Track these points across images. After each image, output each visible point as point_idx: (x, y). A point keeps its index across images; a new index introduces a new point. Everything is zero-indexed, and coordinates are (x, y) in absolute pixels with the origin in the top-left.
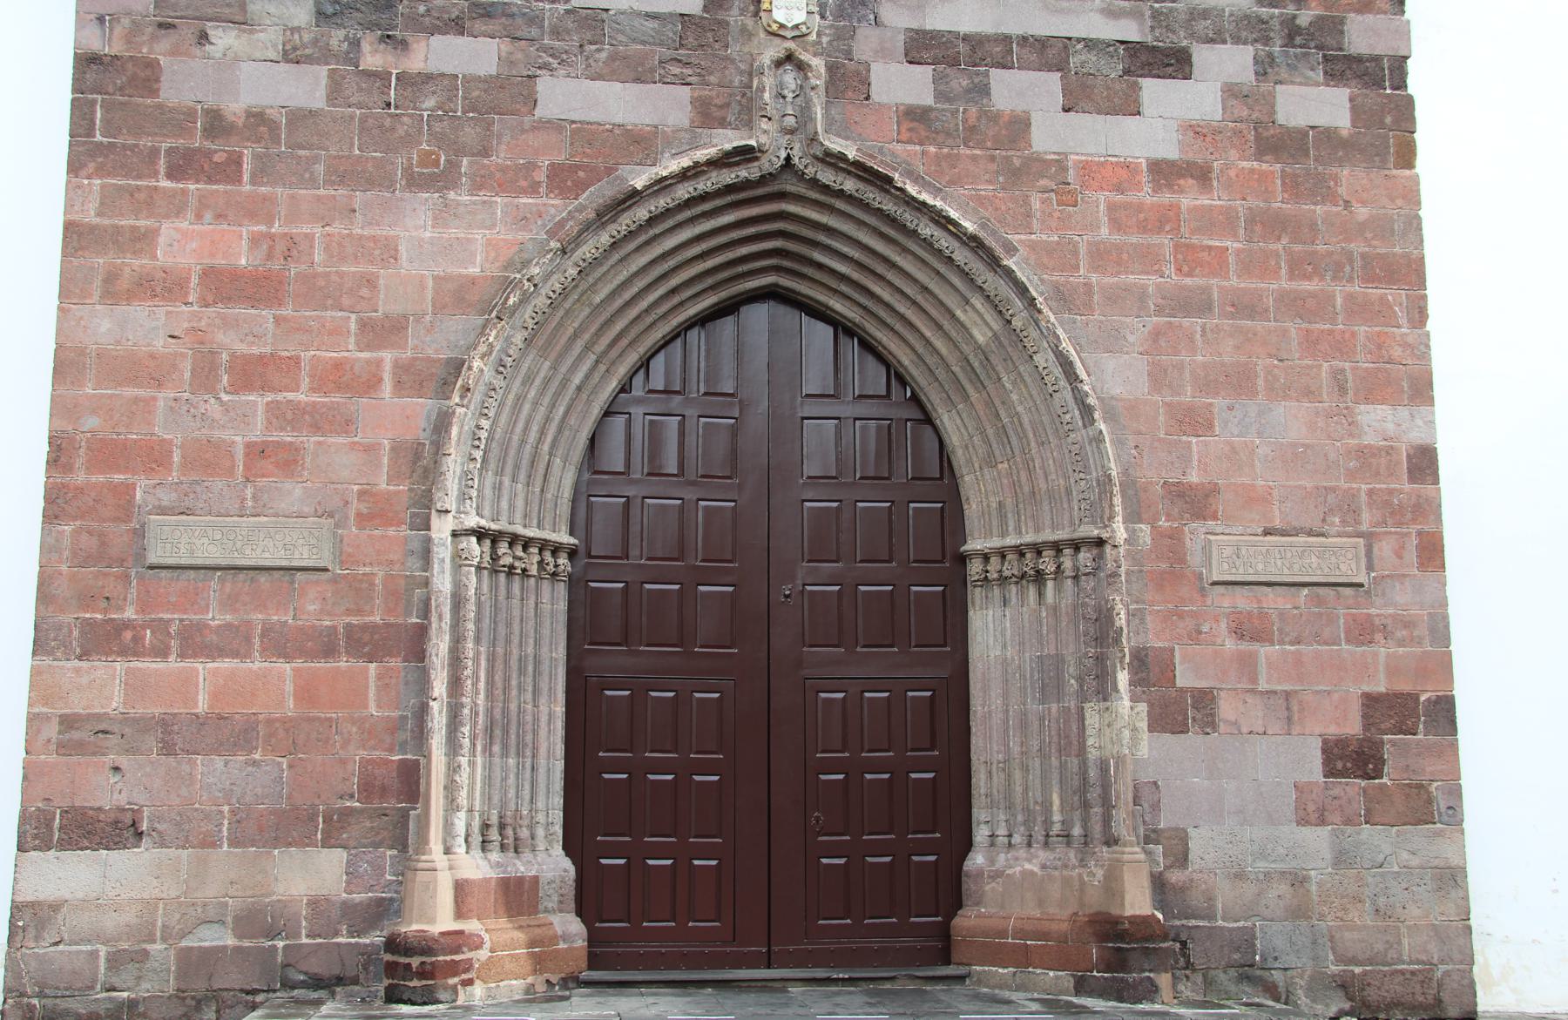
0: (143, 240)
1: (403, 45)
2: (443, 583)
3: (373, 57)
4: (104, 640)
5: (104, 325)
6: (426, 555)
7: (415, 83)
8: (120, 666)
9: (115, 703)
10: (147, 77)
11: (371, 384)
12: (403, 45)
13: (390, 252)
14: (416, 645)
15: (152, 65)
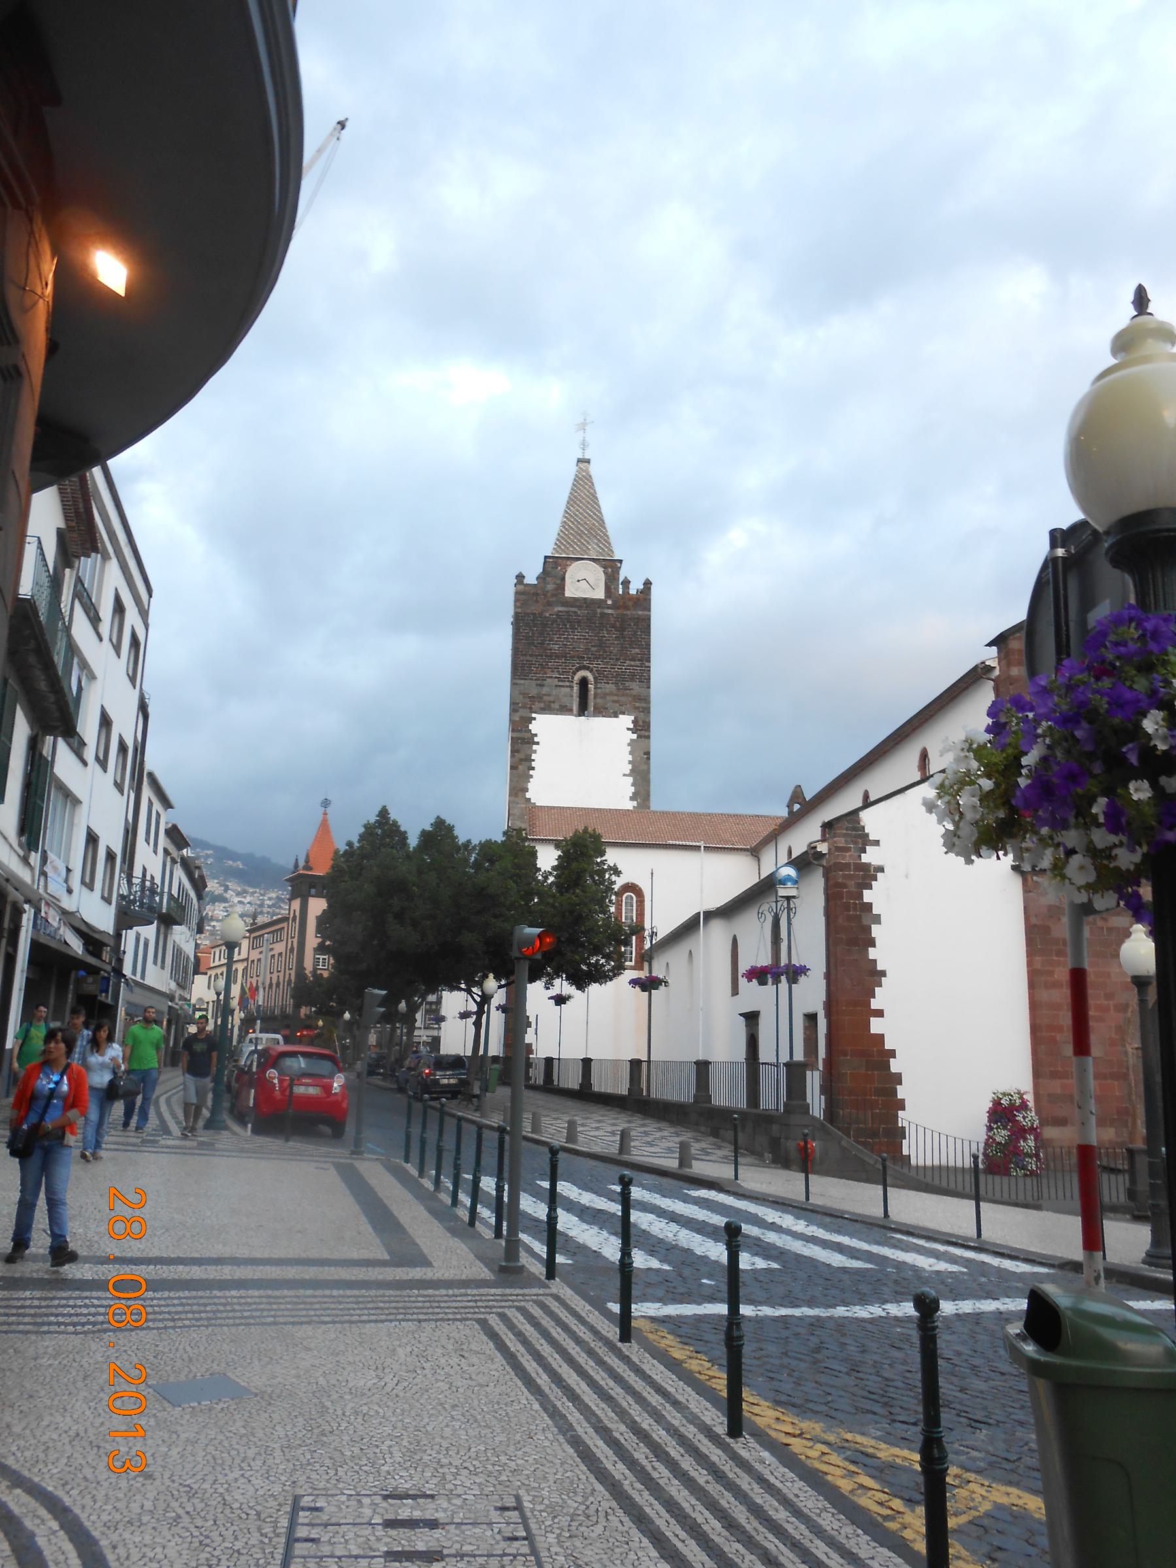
0: (1051, 973)
1: (1105, 920)
2: (1131, 1062)
3: (1100, 923)
4: (1054, 1075)
5: (1044, 995)
6: (1126, 1053)
7: (1110, 929)
8: (1058, 1082)
9: (1059, 1091)
10: (1047, 930)
11: (1108, 1010)
12: (1105, 920)
13: (1108, 975)
14: (1125, 1077)
15: (1049, 927)
